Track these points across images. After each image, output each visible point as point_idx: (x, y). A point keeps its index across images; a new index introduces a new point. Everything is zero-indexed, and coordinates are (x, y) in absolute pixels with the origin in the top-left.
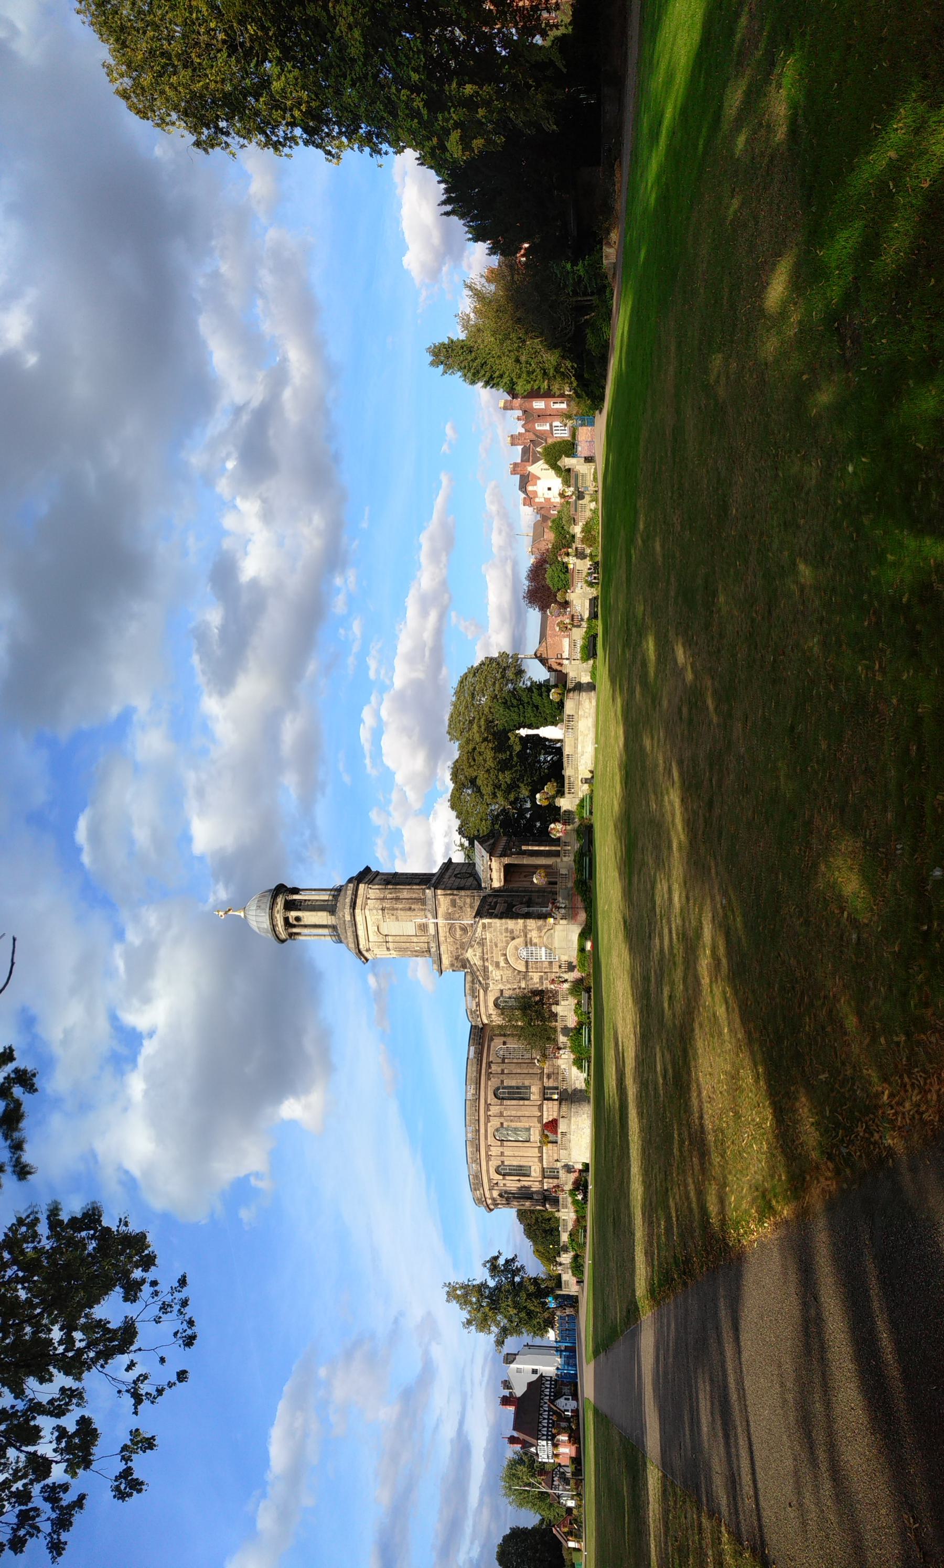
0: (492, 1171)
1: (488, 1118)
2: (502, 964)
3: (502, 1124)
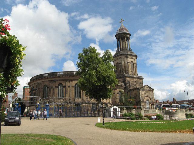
2: (145, 95)
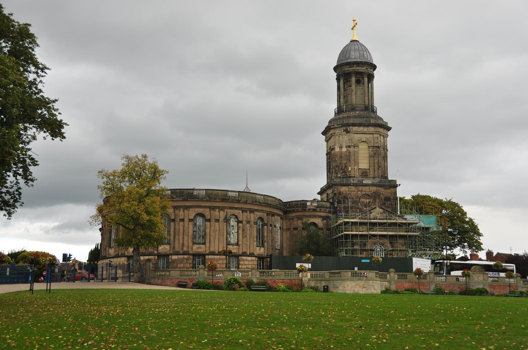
0: (200, 210)
1: (244, 210)
3: (241, 222)
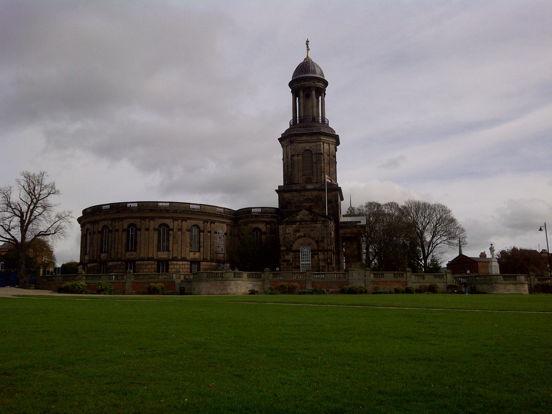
0: (132, 221)
2: (298, 234)
3: (172, 230)
